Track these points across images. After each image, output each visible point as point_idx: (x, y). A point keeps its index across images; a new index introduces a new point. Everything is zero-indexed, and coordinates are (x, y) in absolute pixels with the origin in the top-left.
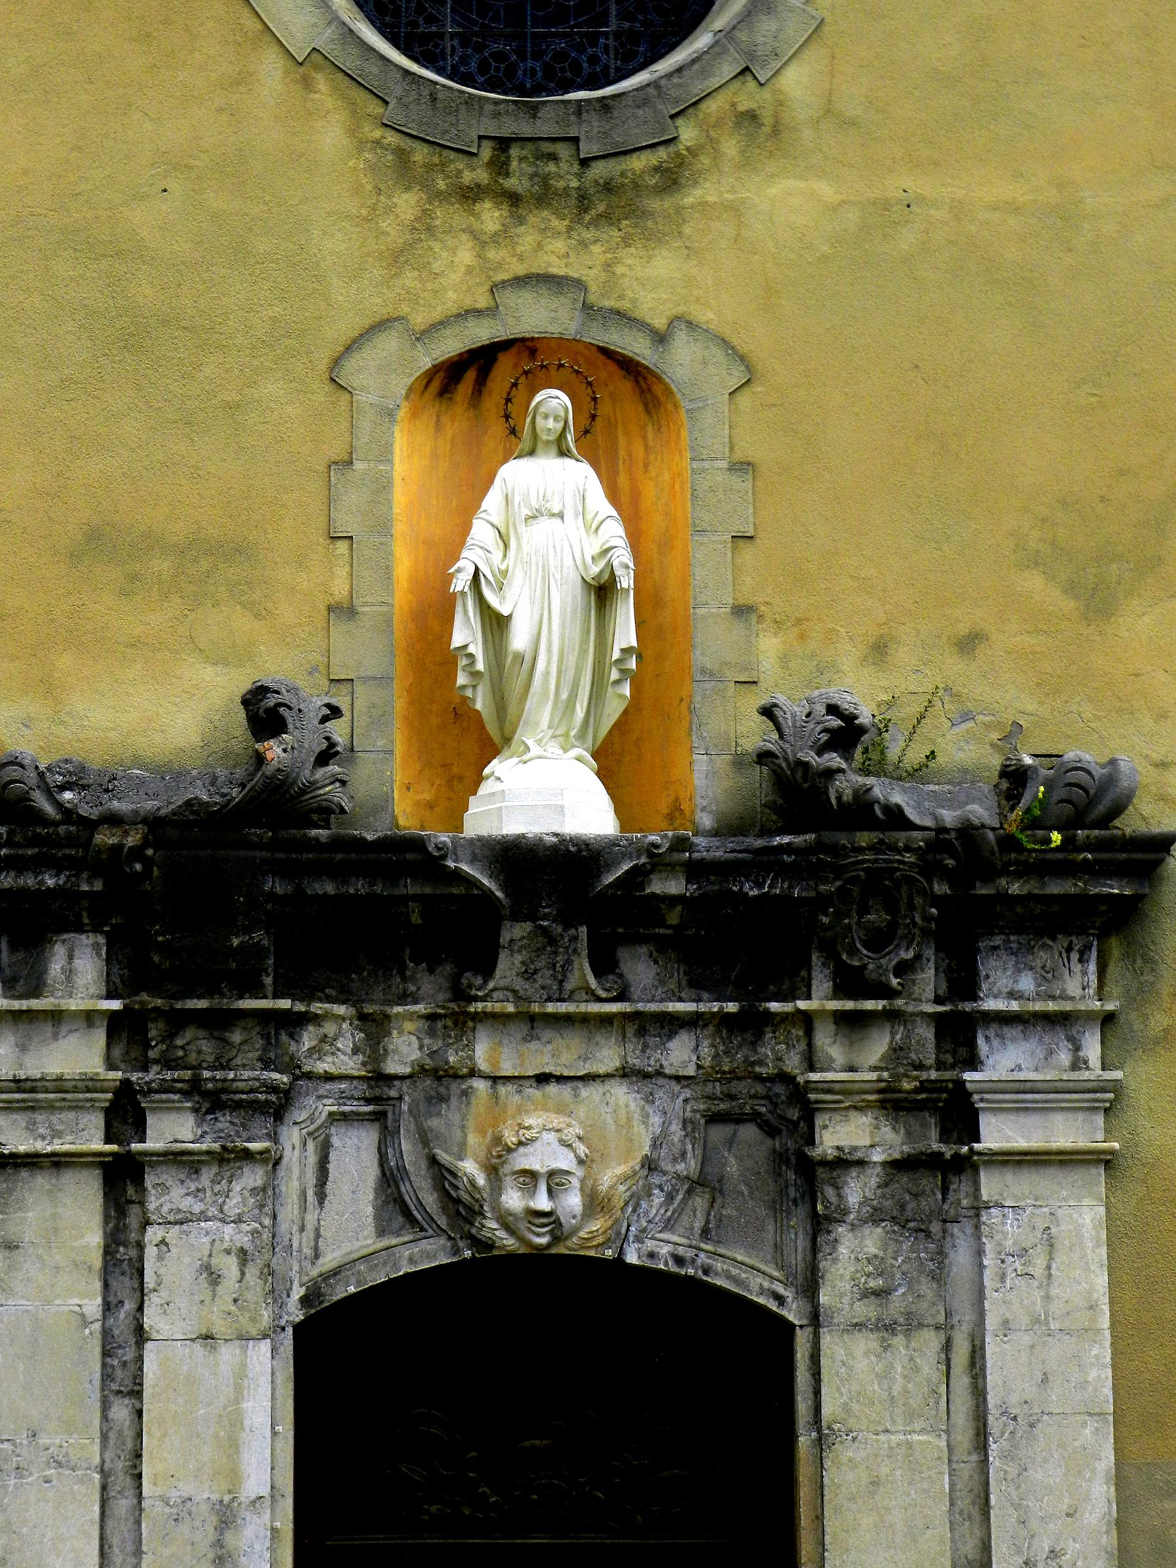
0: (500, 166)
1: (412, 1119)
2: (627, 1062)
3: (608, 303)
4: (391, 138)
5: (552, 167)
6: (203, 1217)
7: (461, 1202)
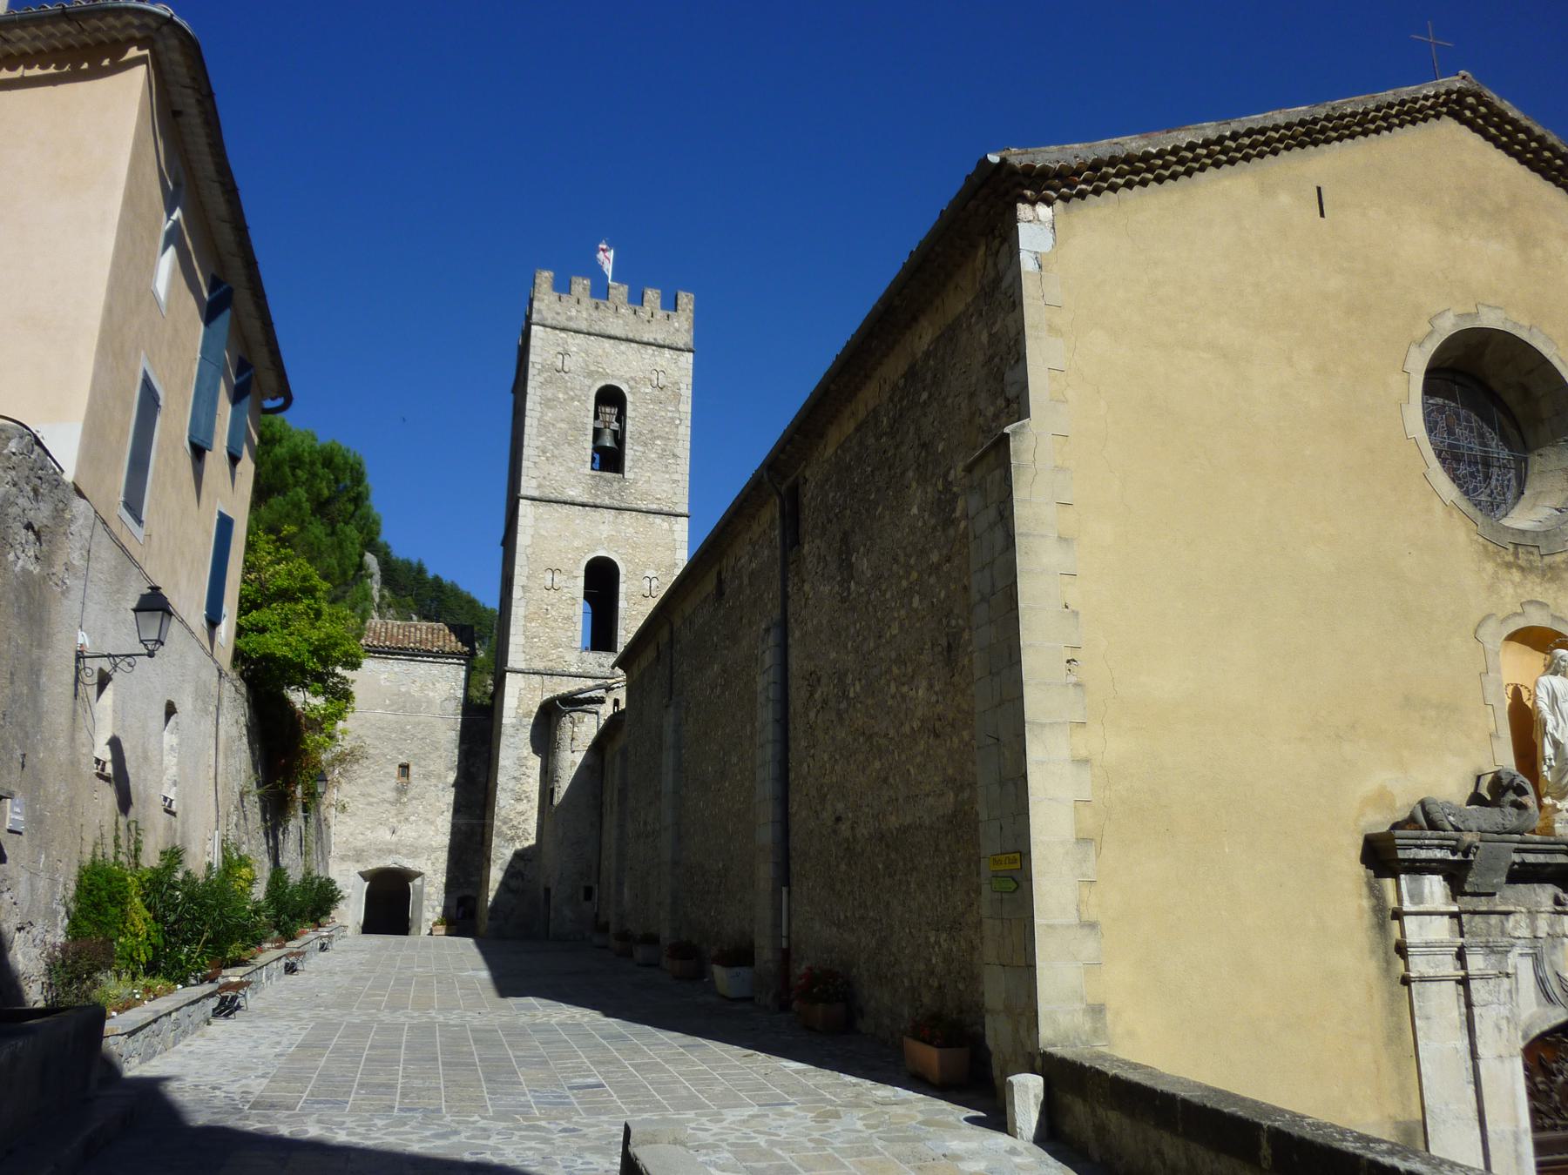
0: (1516, 555)
3: (1558, 614)
4: (1481, 540)
5: (1531, 557)
6: (1492, 1003)
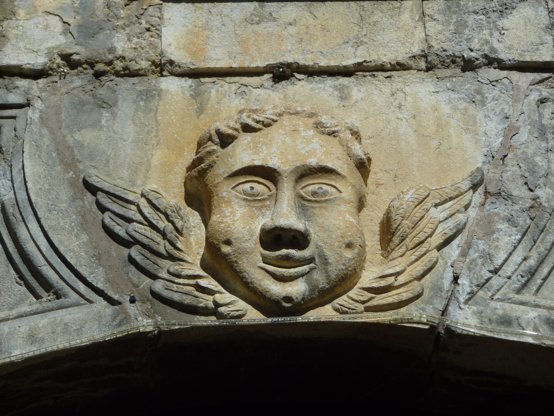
1: (45, 131)
2: (430, 47)
7: (137, 242)
